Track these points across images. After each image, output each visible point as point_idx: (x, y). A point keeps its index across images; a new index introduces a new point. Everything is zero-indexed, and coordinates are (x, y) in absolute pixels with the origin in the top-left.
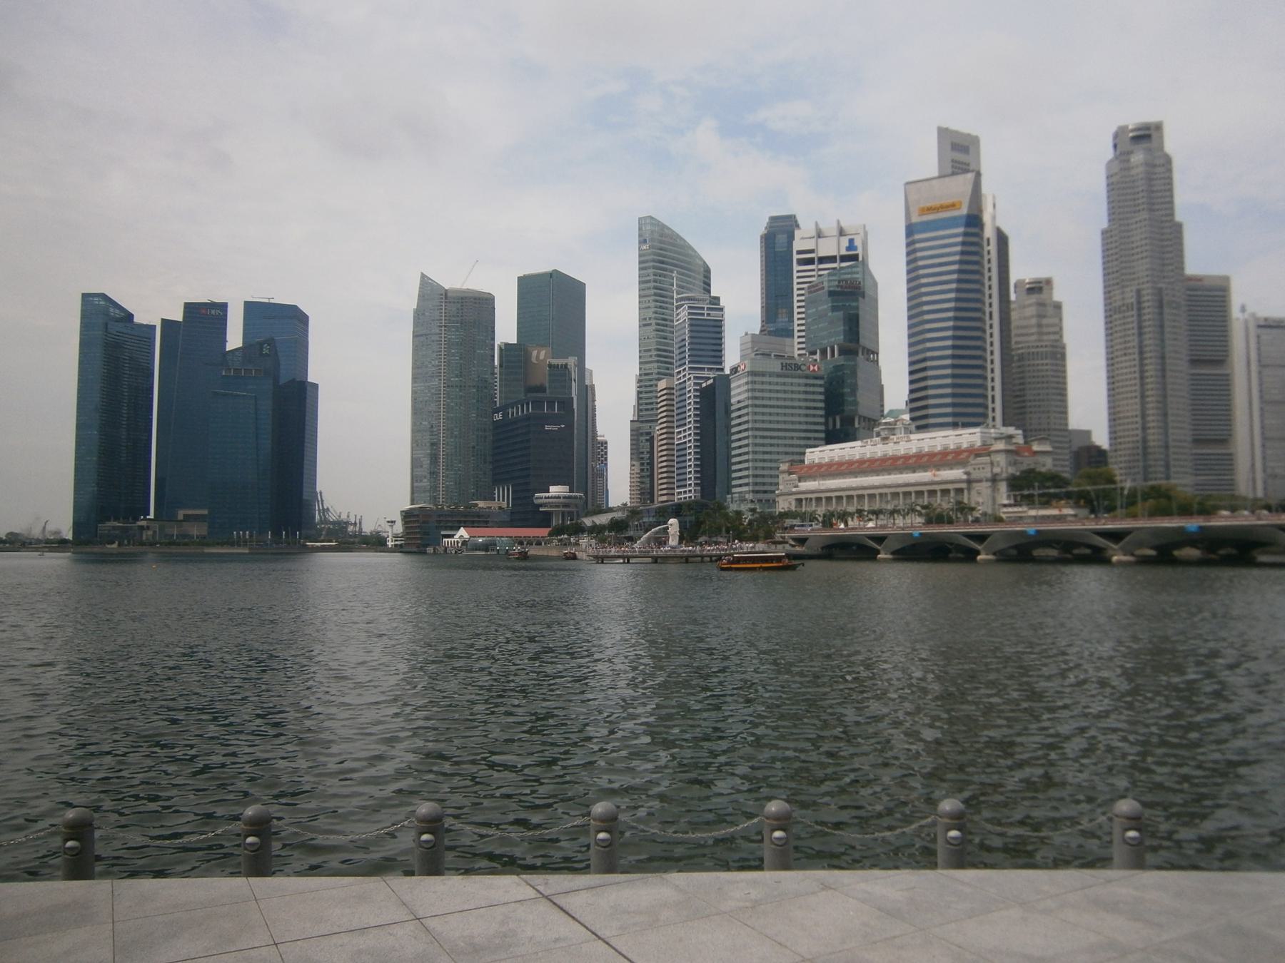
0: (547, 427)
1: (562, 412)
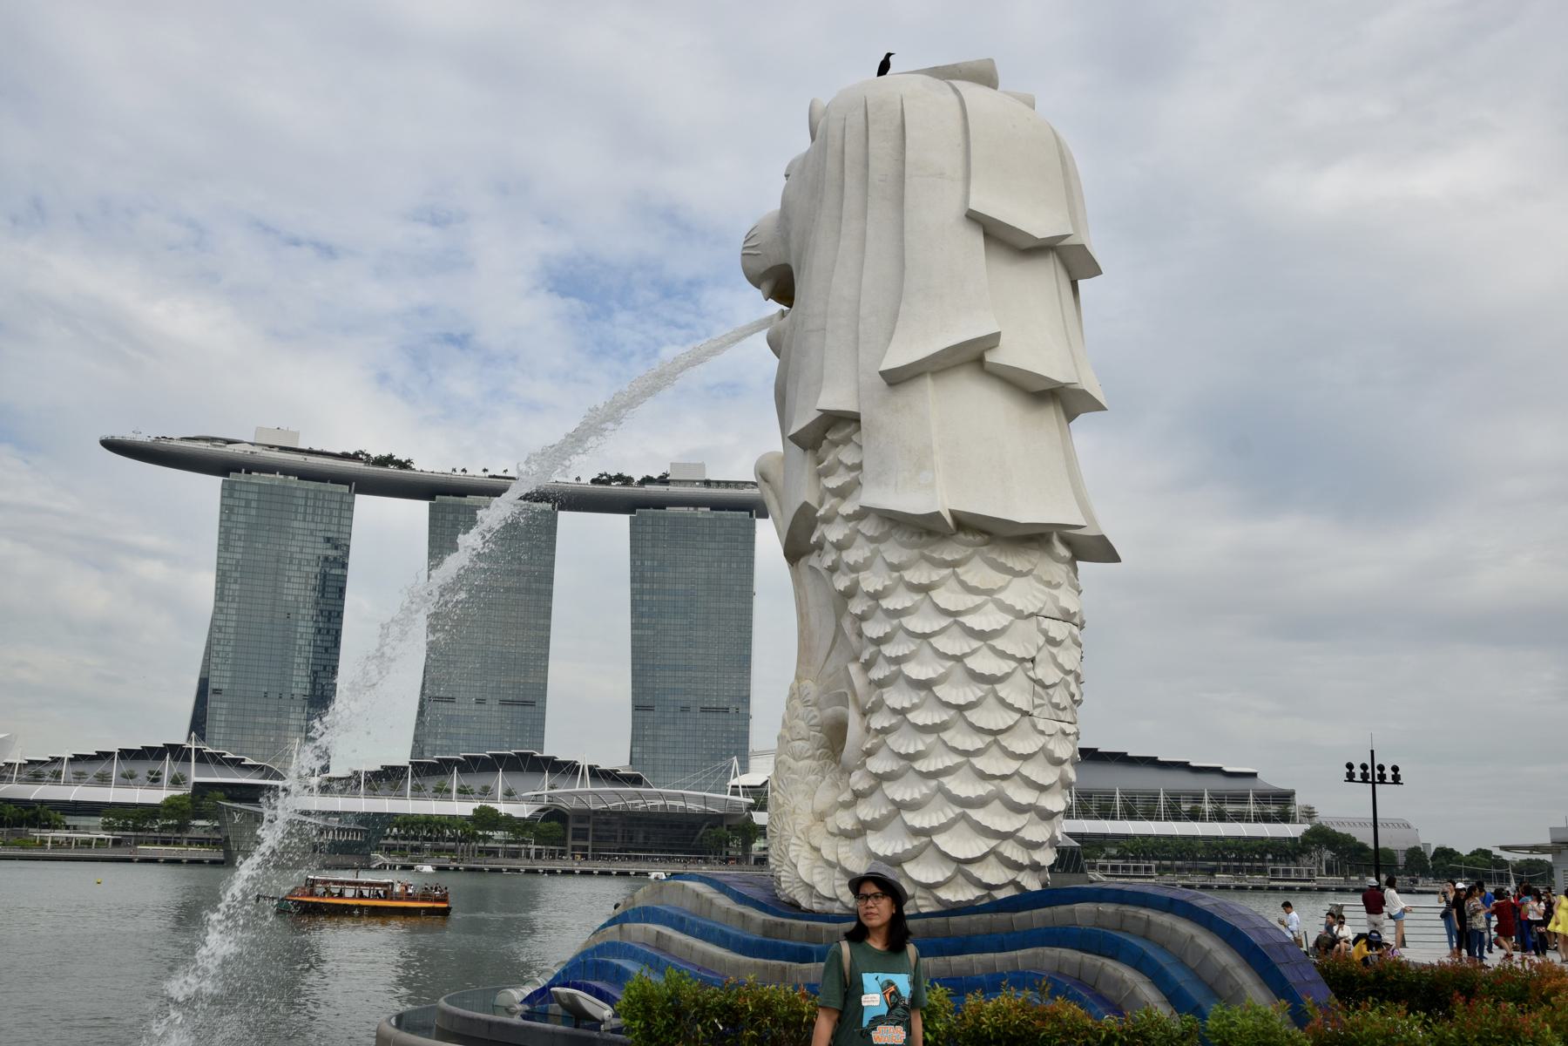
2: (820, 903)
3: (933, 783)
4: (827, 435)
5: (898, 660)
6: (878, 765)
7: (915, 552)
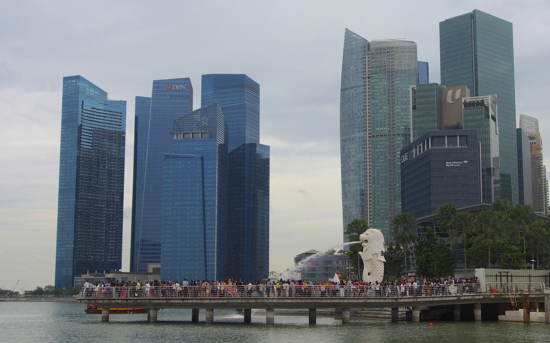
0: (448, 164)
1: (466, 147)
6: (378, 275)
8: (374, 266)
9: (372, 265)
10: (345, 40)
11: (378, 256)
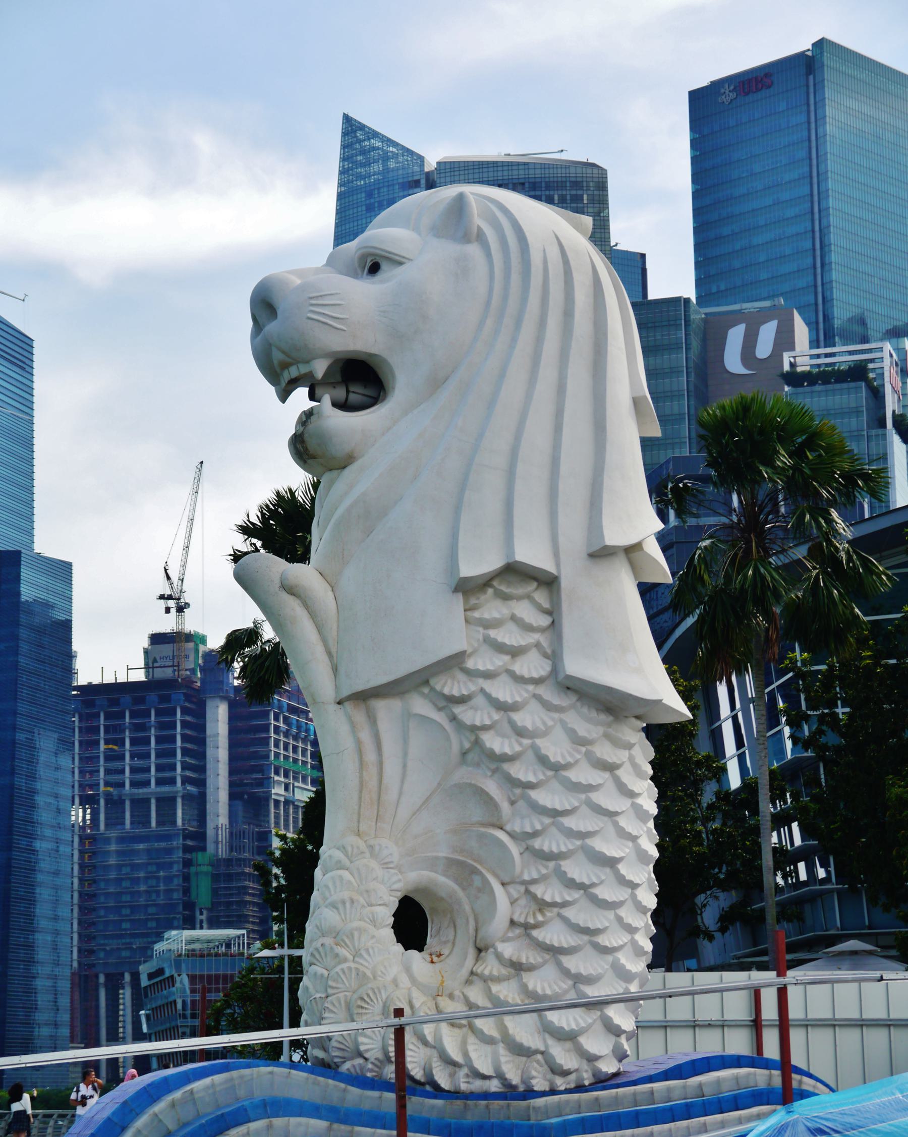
2: (468, 1082)
3: (610, 958)
4: (495, 583)
5: (583, 835)
7: (601, 730)
8: (492, 787)
9: (463, 774)
10: (343, 159)
11: (553, 612)
